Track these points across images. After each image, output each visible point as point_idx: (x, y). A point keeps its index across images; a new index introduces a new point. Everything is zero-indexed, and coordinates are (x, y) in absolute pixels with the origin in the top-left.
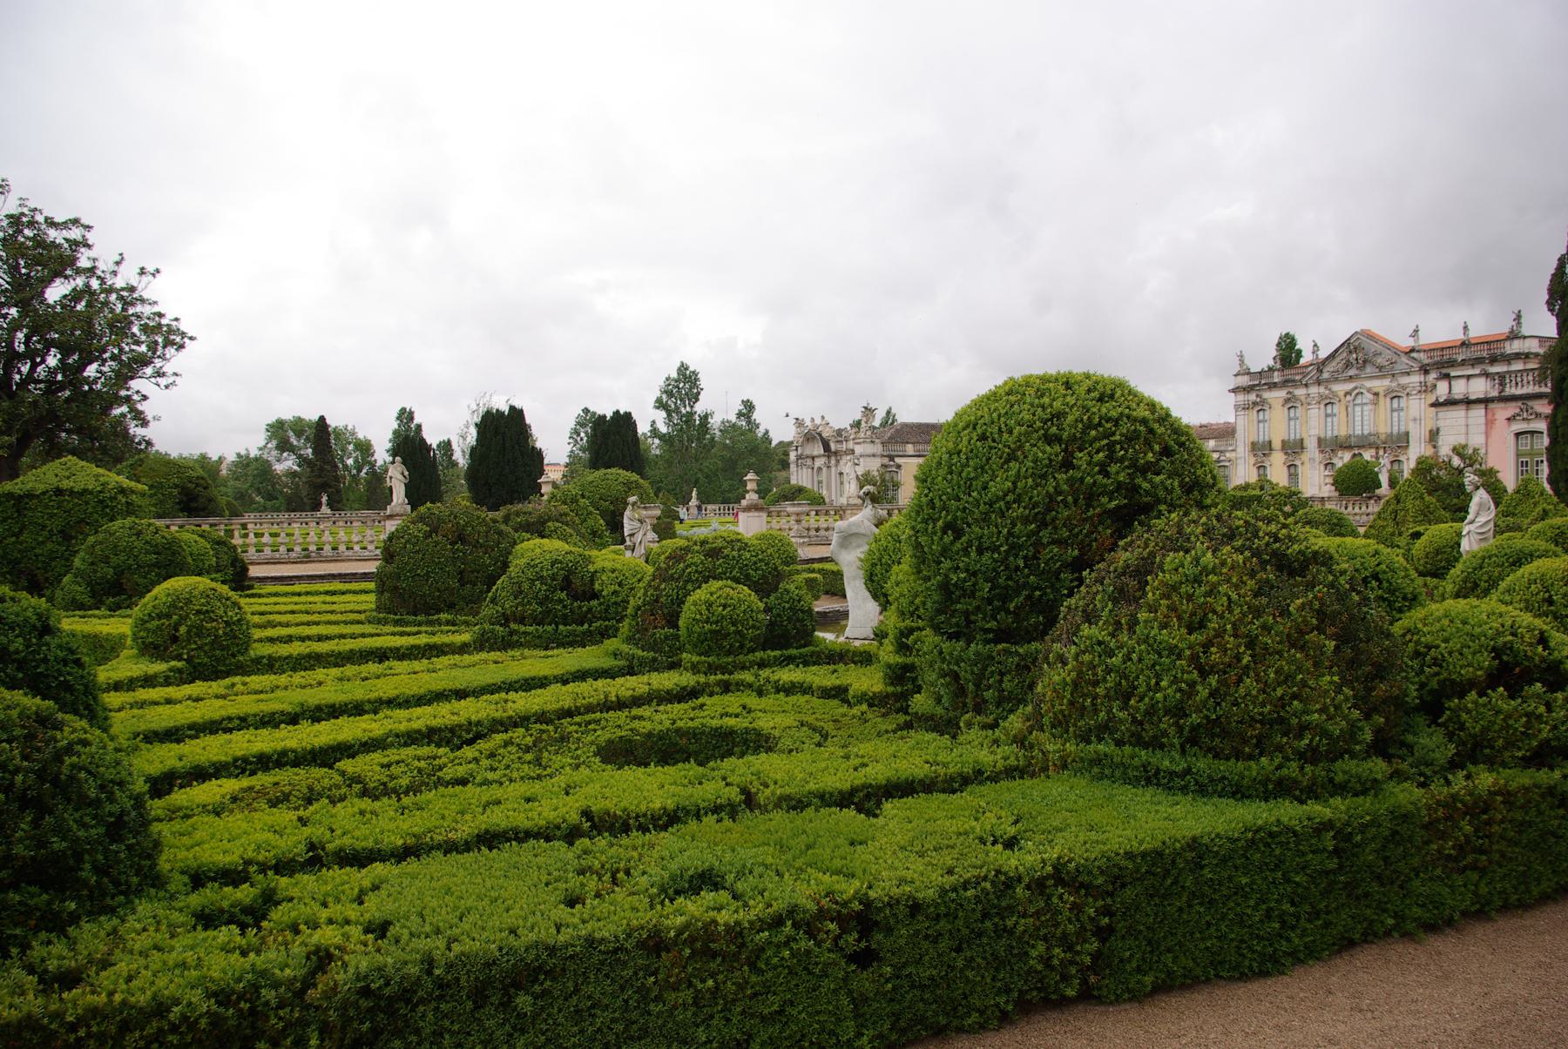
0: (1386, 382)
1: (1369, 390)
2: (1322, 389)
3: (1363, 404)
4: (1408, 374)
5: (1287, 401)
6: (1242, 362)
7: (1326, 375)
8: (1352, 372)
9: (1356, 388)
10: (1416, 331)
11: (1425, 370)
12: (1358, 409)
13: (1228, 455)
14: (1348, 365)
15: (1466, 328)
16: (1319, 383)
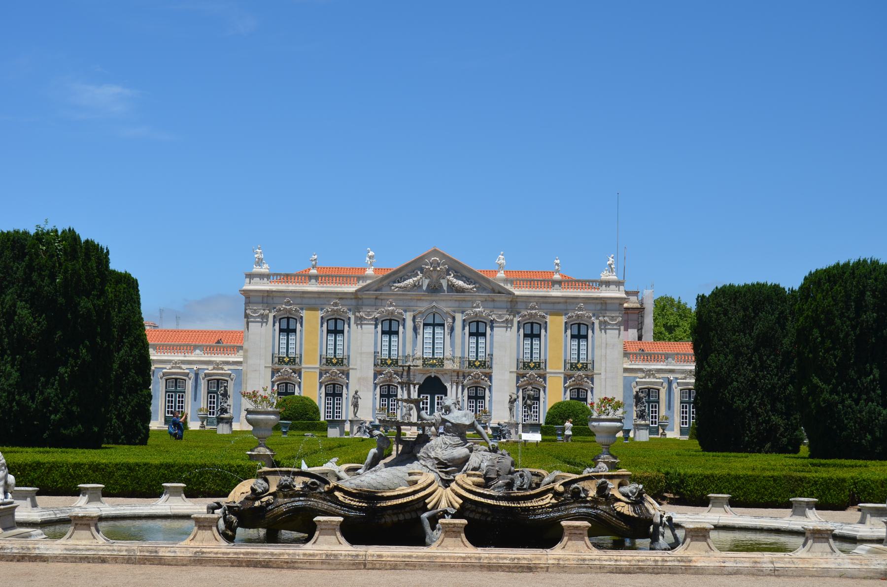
3: (434, 325)
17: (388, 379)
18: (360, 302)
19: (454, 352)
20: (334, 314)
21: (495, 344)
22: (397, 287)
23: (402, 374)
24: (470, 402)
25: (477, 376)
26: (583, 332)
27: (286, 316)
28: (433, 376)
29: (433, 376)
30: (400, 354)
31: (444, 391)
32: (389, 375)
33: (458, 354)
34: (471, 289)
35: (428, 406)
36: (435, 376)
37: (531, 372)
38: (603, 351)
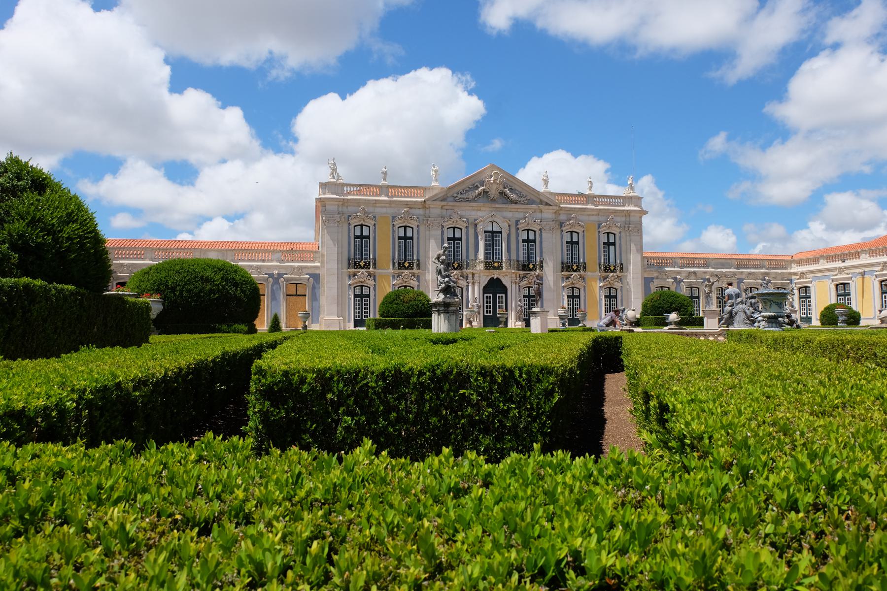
3: (493, 232)
6: (334, 170)
18: (427, 211)
19: (510, 256)
20: (404, 222)
21: (544, 250)
23: (467, 277)
25: (531, 277)
26: (612, 240)
27: (360, 223)
30: (464, 258)
31: (504, 290)
32: (456, 277)
33: (514, 257)
36: (497, 278)
37: (575, 274)
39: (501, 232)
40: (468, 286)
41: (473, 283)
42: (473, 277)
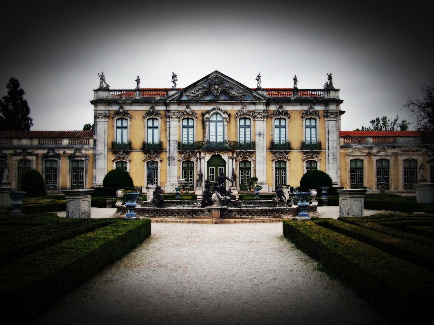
0: (238, 108)
1: (225, 112)
2: (182, 108)
3: (217, 121)
4: (255, 104)
5: (149, 113)
7: (184, 98)
8: (208, 98)
9: (214, 109)
10: (259, 77)
11: (268, 104)
12: (213, 124)
13: (83, 152)
14: (208, 92)
15: (295, 80)
16: (180, 102)
17: (187, 157)
22: (192, 97)
23: (197, 154)
24: (241, 171)
28: (216, 154)
29: (216, 154)
31: (224, 163)
34: (240, 97)
35: (214, 174)
36: (218, 154)
38: (327, 135)
39: (222, 121)
40: (197, 161)
41: (200, 159)
42: (200, 154)
